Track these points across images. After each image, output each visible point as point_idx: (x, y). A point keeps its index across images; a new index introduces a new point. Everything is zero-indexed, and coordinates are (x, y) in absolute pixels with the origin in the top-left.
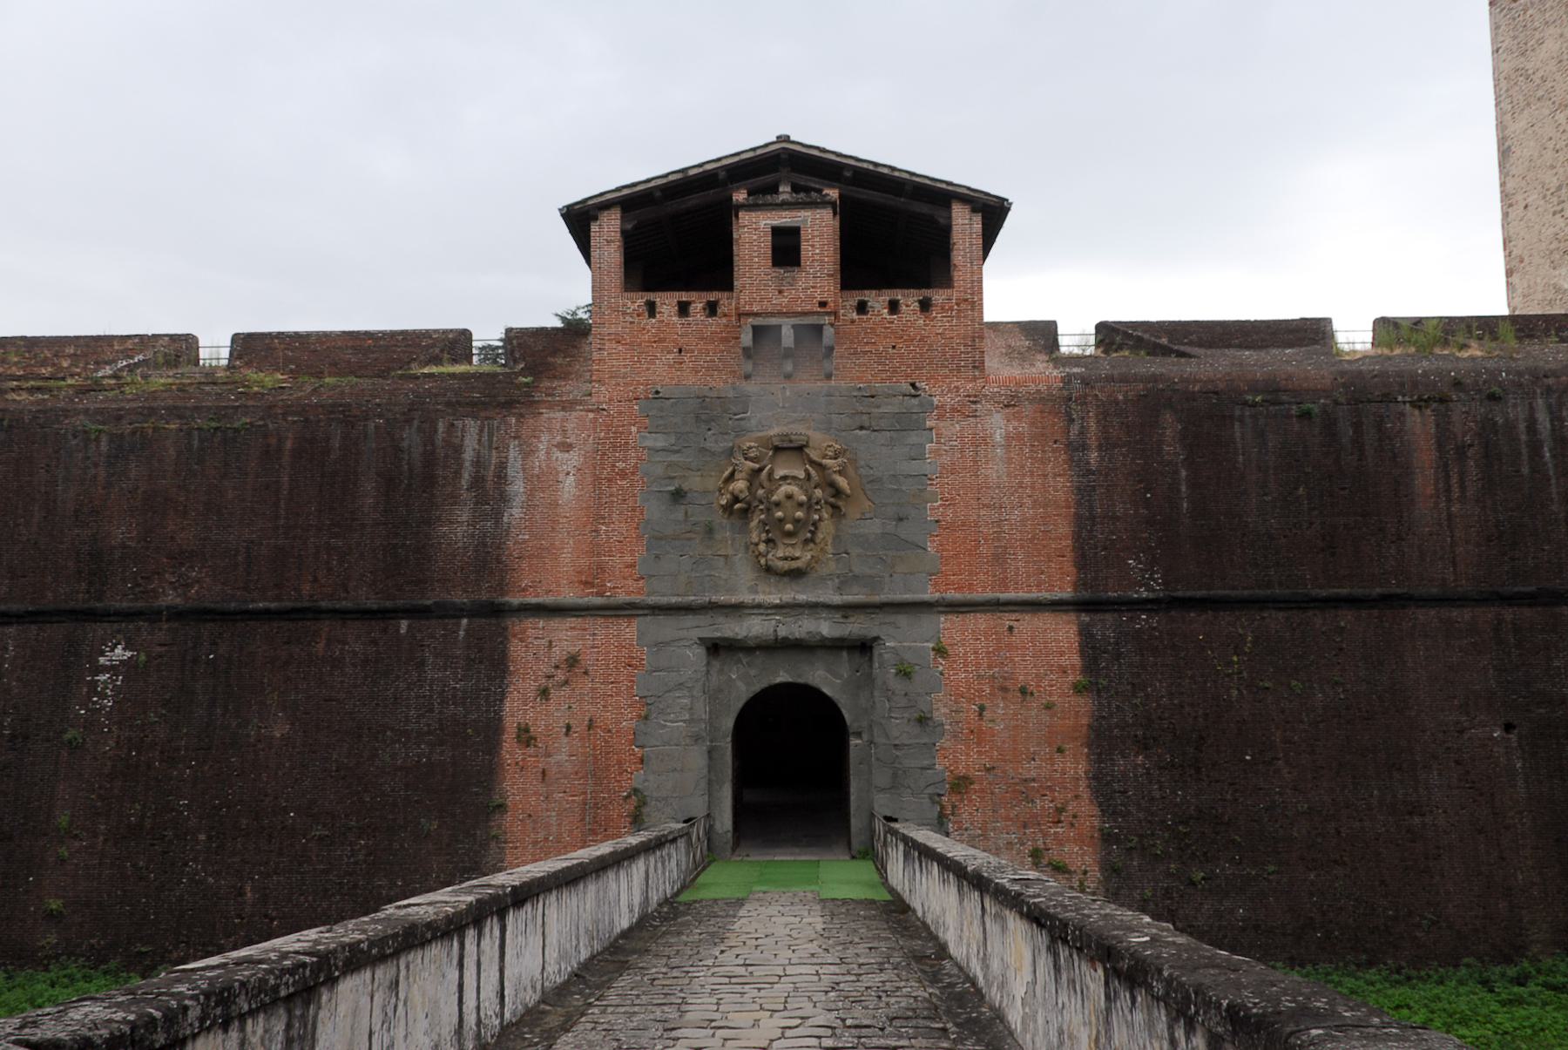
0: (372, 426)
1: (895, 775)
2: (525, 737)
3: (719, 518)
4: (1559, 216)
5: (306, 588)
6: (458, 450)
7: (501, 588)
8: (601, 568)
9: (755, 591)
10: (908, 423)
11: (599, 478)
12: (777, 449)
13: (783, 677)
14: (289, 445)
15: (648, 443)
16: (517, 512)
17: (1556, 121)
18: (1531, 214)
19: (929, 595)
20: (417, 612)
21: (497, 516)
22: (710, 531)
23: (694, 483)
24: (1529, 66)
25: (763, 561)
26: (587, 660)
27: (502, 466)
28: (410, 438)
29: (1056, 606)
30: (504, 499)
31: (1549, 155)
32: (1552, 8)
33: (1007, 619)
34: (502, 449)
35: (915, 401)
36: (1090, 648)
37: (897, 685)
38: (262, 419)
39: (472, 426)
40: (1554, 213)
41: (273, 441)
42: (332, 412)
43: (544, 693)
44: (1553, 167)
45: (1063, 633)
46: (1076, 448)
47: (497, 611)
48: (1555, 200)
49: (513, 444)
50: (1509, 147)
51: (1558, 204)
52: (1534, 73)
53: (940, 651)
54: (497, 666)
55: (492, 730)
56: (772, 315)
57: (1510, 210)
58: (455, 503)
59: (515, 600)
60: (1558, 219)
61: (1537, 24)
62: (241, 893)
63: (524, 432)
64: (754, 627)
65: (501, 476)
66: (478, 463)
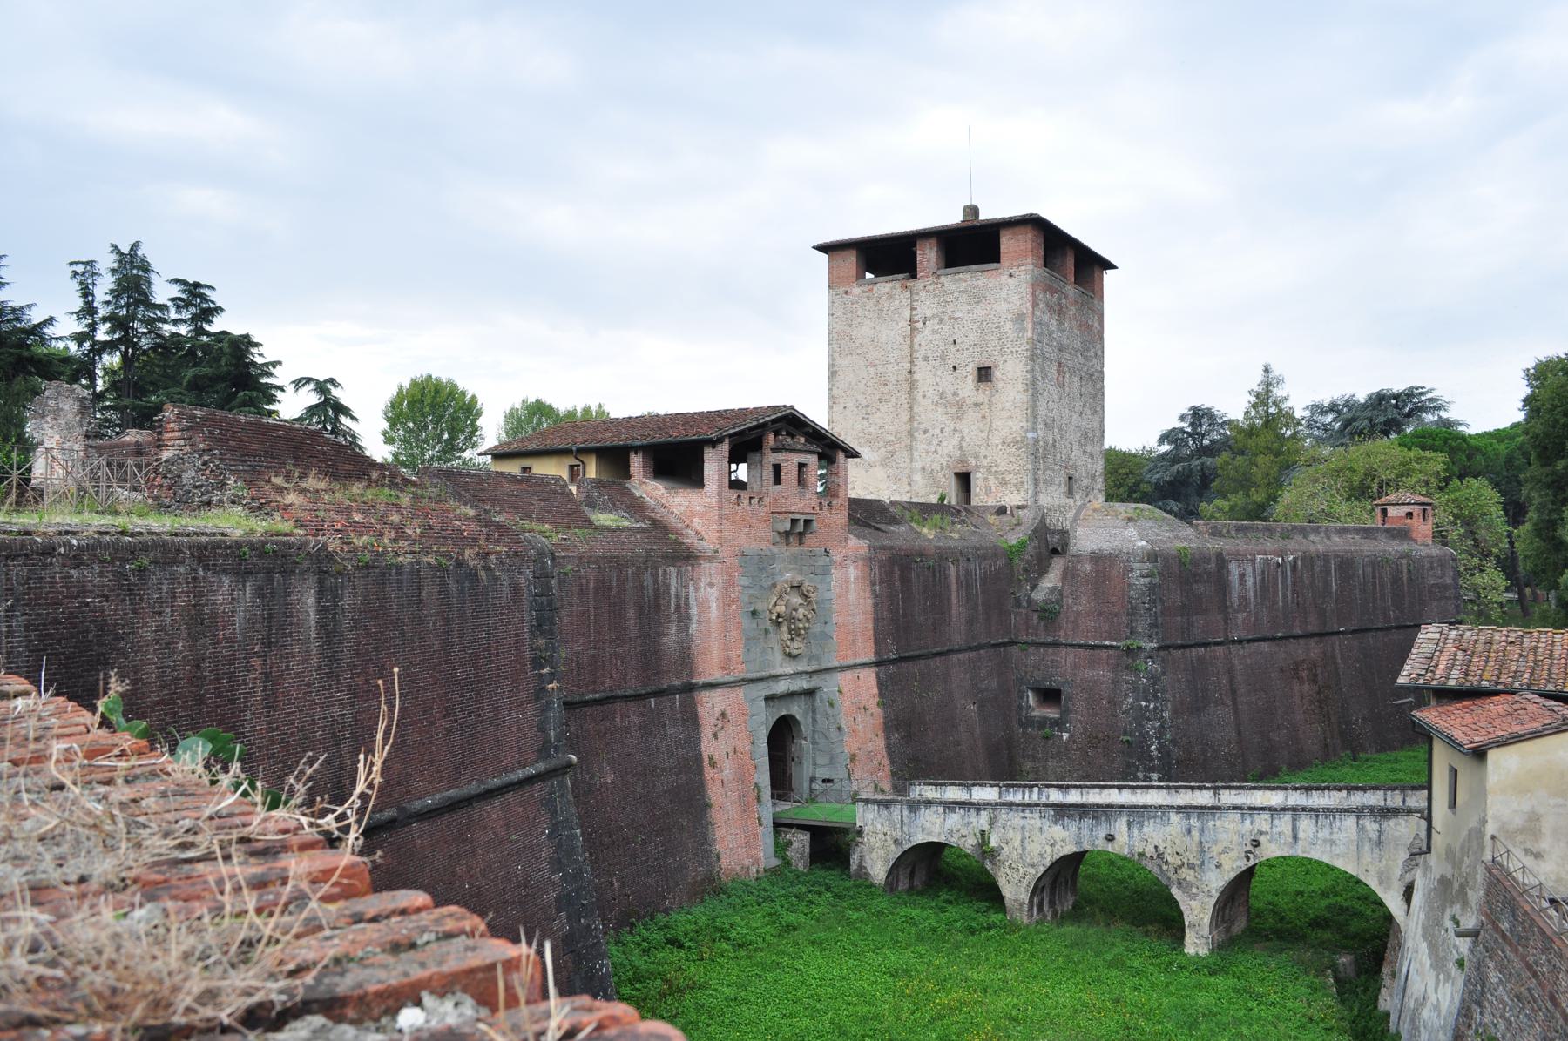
0: (630, 572)
1: (832, 758)
2: (713, 764)
3: (768, 625)
5: (607, 682)
6: (668, 587)
7: (691, 675)
8: (729, 658)
9: (781, 666)
10: (826, 572)
11: (727, 603)
12: (792, 587)
13: (784, 713)
14: (592, 585)
15: (742, 583)
16: (694, 626)
18: (847, 412)
19: (836, 664)
20: (659, 693)
21: (687, 628)
22: (766, 632)
23: (759, 607)
24: (854, 334)
25: (788, 650)
26: (728, 712)
27: (687, 598)
28: (647, 579)
29: (864, 665)
30: (689, 619)
31: (862, 386)
33: (857, 672)
34: (687, 587)
35: (828, 559)
36: (880, 684)
37: (829, 710)
38: (577, 566)
39: (673, 571)
41: (584, 581)
42: (611, 562)
43: (715, 735)
45: (869, 677)
46: (873, 584)
47: (691, 688)
49: (691, 583)
50: (836, 372)
53: (840, 692)
54: (691, 720)
55: (698, 759)
56: (798, 513)
58: (669, 622)
59: (700, 680)
60: (865, 422)
61: (859, 314)
62: (612, 885)
63: (695, 576)
64: (781, 687)
65: (687, 604)
66: (677, 596)
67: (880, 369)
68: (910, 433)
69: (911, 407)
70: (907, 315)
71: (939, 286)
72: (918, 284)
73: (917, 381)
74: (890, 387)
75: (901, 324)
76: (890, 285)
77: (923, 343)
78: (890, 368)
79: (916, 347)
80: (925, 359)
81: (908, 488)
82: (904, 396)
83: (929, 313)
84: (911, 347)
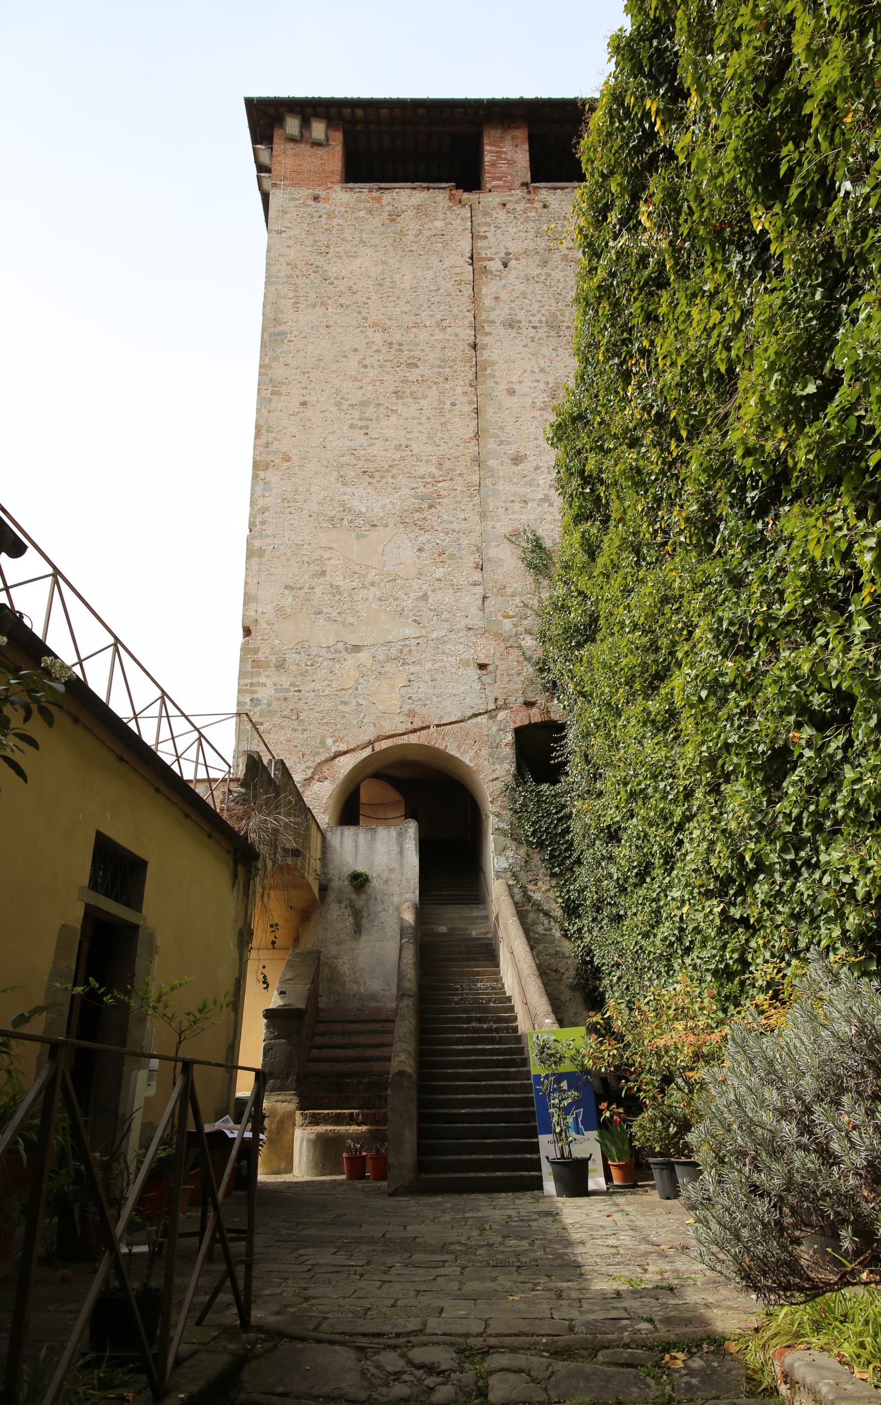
4: (357, 431)
17: (366, 337)
24: (332, 271)
31: (352, 365)
32: (373, 232)
40: (352, 426)
44: (356, 379)
48: (356, 414)
51: (360, 419)
52: (337, 278)
57: (275, 398)
67: (397, 337)
68: (478, 461)
69: (477, 411)
70: (465, 245)
71: (538, 205)
72: (488, 199)
73: (493, 363)
74: (424, 370)
75: (448, 262)
76: (424, 194)
77: (504, 296)
78: (423, 335)
79: (488, 302)
80: (511, 324)
81: (477, 576)
82: (459, 388)
83: (515, 247)
84: (475, 299)
